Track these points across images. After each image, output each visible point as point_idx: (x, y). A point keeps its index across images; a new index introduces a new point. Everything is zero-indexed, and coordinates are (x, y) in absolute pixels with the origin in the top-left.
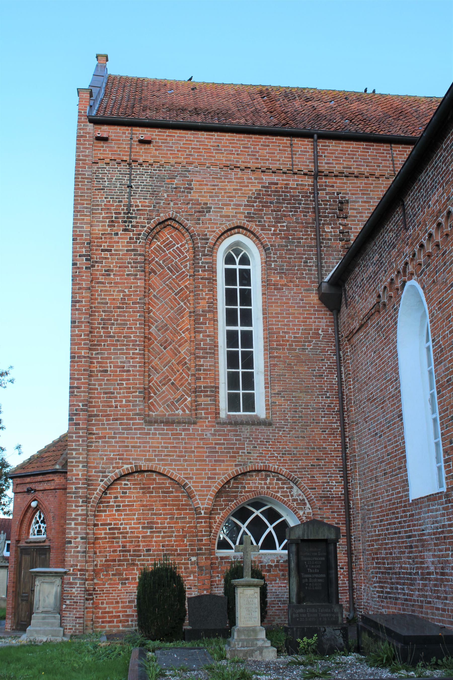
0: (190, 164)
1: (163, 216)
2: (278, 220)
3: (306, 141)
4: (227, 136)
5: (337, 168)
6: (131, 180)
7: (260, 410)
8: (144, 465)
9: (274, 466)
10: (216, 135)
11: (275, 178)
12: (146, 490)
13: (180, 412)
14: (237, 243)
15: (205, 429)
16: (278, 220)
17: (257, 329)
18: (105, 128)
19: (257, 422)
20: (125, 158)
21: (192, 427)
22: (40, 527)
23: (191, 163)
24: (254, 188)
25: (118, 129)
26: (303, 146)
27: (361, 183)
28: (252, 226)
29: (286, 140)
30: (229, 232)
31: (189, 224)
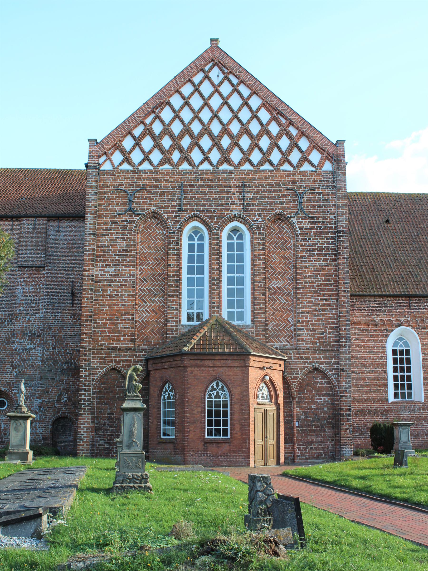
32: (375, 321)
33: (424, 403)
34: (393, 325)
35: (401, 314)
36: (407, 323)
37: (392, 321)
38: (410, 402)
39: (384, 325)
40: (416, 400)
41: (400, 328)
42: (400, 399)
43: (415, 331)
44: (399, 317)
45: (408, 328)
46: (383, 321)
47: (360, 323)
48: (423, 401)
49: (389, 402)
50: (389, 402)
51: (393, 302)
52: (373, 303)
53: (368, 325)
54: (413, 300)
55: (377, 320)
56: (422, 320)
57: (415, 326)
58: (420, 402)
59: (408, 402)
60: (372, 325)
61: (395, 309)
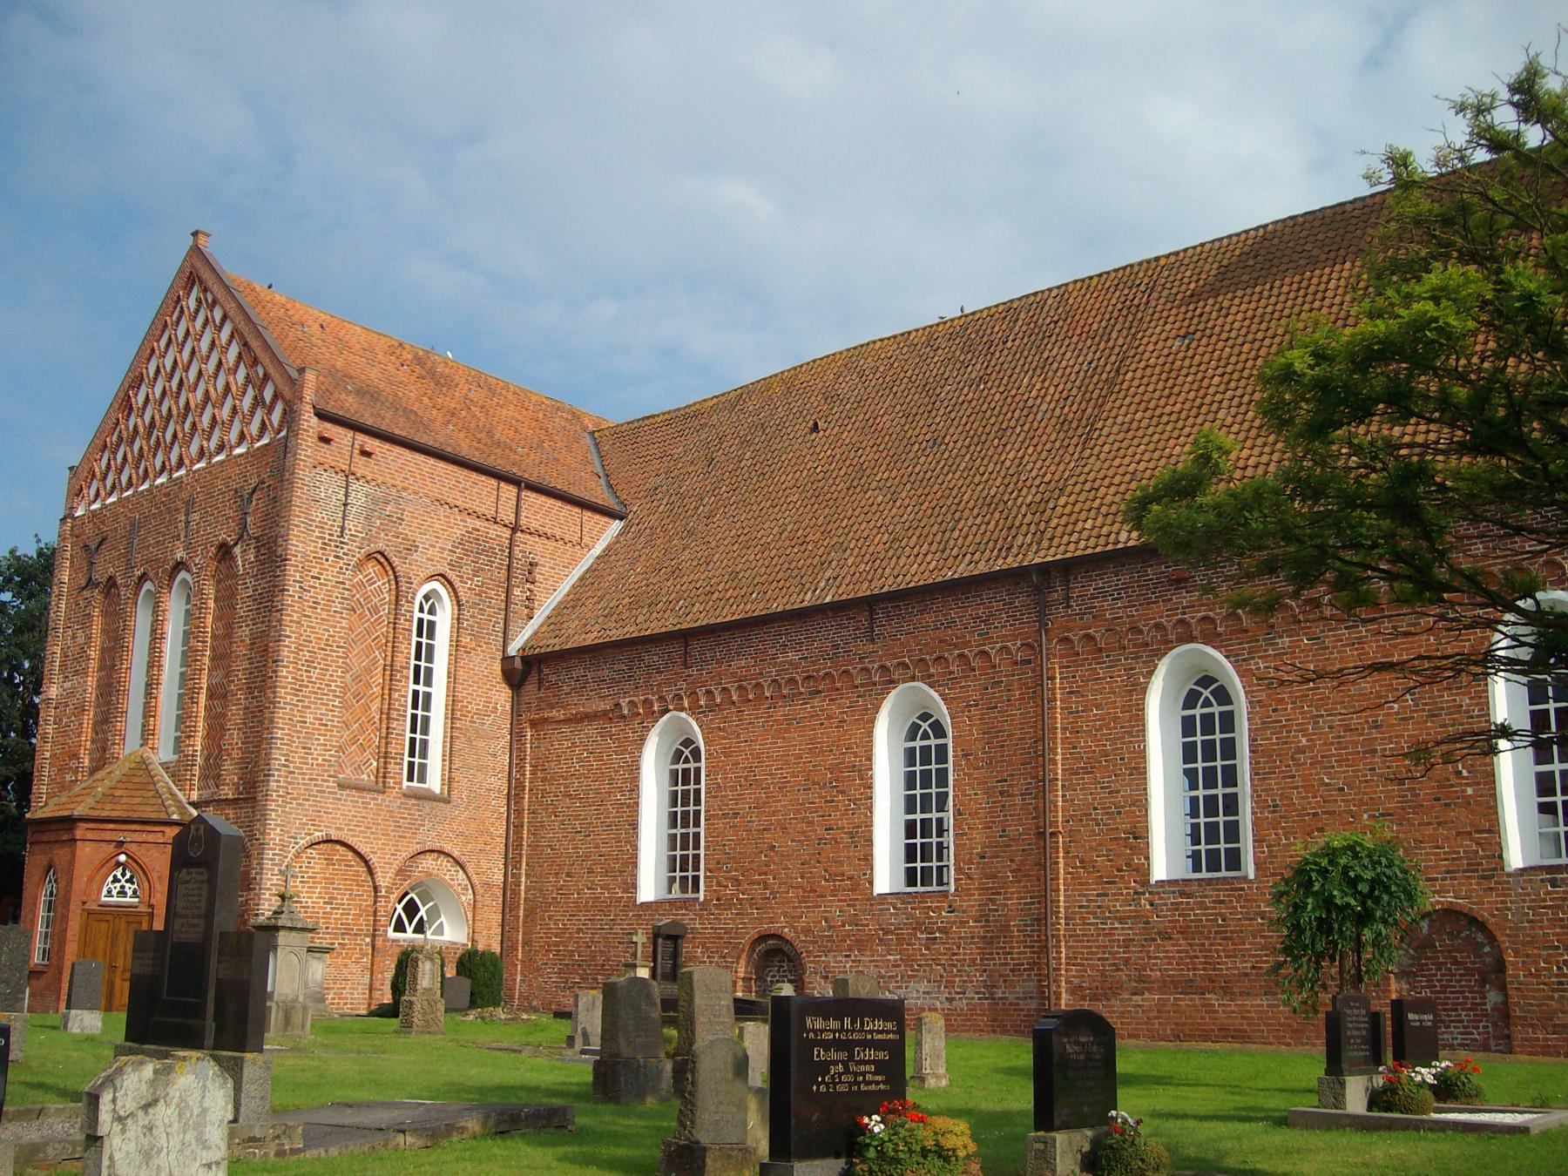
0: (405, 489)
1: (373, 547)
2: (476, 572)
3: (511, 488)
4: (442, 465)
5: (534, 525)
6: (346, 496)
7: (434, 782)
8: (335, 835)
9: (447, 848)
10: (432, 461)
11: (478, 524)
12: (330, 862)
13: (365, 777)
14: (434, 591)
15: (390, 800)
16: (476, 572)
17: (439, 691)
18: (328, 425)
19: (429, 797)
20: (345, 467)
21: (380, 797)
22: (123, 887)
23: (405, 489)
24: (458, 533)
25: (340, 430)
26: (509, 491)
27: (551, 544)
28: (452, 576)
29: (493, 482)
30: (430, 578)
31: (396, 561)
33: (702, 904)
35: (668, 682)
41: (668, 715)
45: (683, 715)
51: (654, 657)
54: (695, 645)
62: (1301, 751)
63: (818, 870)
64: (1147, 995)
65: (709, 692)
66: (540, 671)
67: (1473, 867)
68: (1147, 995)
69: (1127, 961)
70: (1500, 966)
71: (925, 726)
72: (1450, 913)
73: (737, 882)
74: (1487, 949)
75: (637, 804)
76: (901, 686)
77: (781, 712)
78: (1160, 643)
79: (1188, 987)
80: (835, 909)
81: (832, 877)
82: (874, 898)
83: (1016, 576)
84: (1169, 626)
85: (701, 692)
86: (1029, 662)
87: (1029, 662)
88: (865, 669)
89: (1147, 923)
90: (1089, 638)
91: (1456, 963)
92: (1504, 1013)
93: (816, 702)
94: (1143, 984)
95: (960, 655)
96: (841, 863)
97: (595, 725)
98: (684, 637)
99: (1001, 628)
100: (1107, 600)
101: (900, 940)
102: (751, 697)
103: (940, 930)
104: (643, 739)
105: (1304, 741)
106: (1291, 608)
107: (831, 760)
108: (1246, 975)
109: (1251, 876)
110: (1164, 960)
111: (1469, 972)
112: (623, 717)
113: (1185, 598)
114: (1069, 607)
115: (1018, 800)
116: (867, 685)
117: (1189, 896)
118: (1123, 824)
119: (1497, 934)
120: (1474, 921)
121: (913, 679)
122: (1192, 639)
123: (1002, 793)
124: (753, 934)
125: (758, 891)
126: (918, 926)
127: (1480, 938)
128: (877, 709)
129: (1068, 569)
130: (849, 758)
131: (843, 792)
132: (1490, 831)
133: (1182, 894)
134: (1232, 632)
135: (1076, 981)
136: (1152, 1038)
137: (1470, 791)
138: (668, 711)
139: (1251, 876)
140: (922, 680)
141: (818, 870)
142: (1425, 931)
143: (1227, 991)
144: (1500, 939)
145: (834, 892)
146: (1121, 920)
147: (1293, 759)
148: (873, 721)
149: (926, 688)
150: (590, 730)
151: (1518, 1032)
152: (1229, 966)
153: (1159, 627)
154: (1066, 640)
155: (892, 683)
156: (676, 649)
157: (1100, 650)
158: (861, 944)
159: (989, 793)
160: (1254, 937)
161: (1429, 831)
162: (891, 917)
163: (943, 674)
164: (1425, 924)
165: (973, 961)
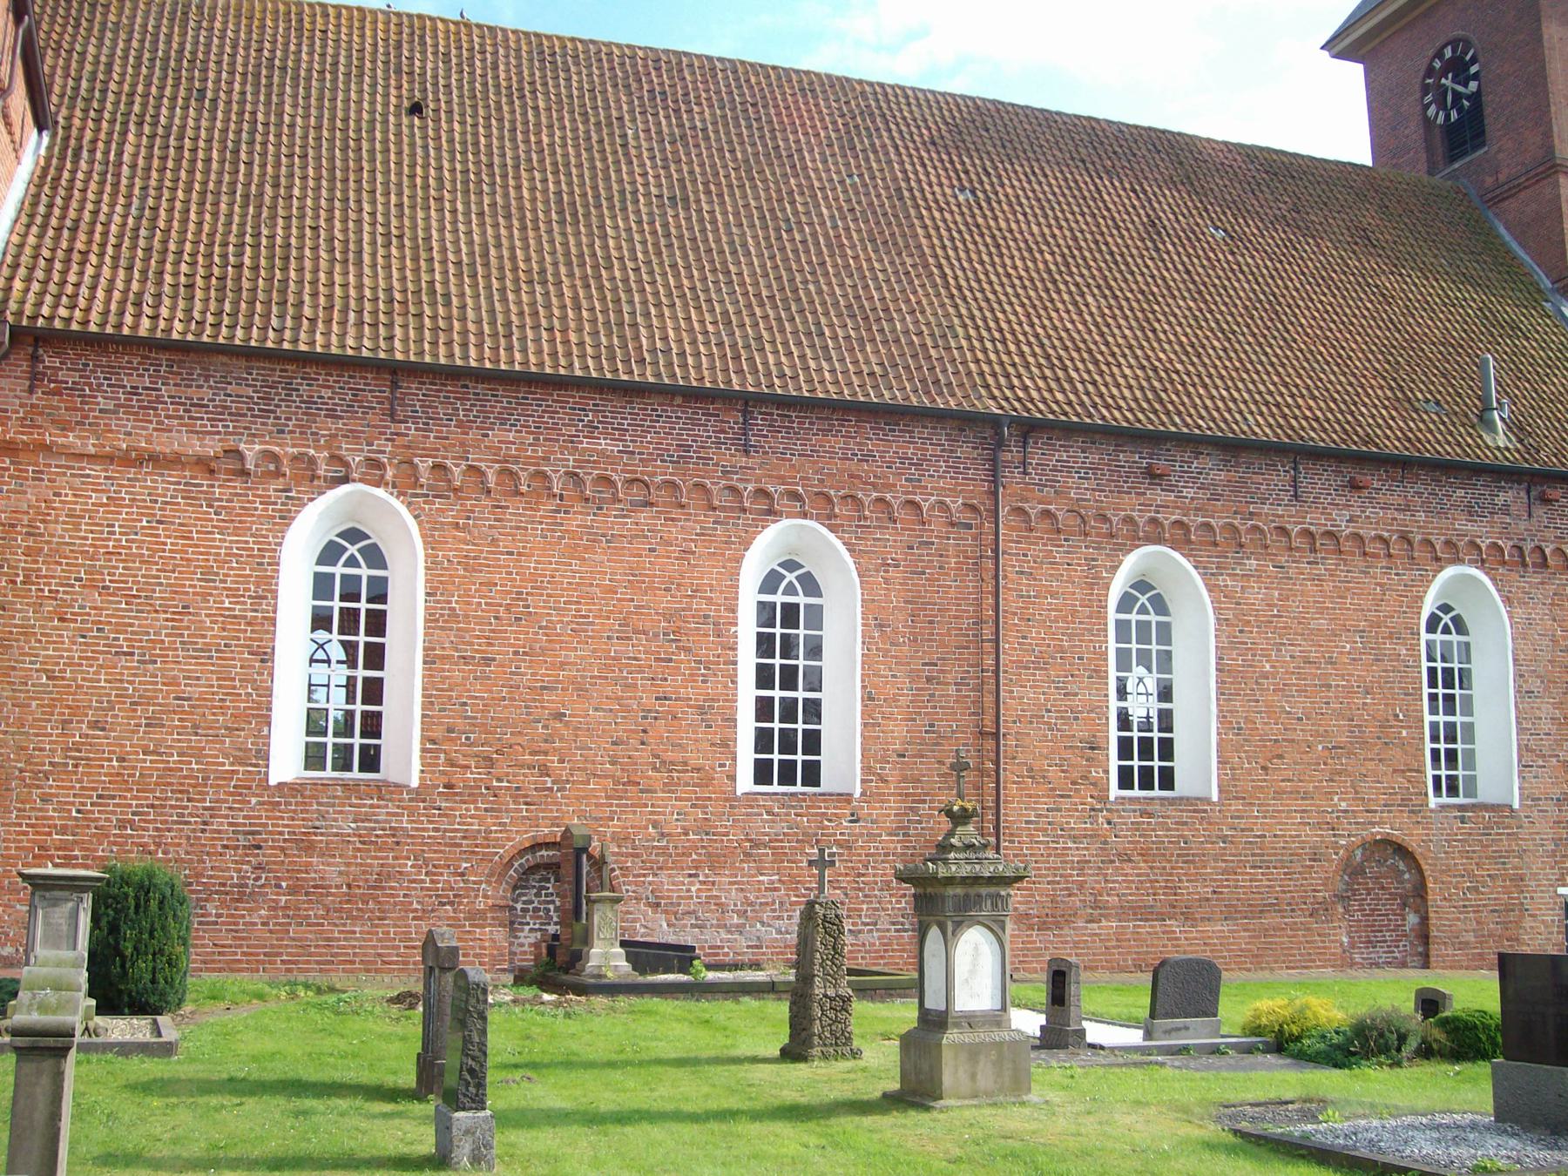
32: (240, 456)
33: (417, 791)
34: (311, 479)
35: (353, 435)
36: (374, 472)
37: (312, 461)
38: (367, 783)
39: (278, 474)
40: (392, 779)
42: (330, 773)
43: (409, 505)
44: (345, 448)
45: (380, 492)
46: (274, 458)
47: (174, 461)
48: (415, 783)
49: (273, 781)
50: (273, 781)
51: (326, 389)
52: (247, 386)
53: (212, 472)
55: (251, 451)
56: (436, 466)
57: (406, 485)
58: (400, 787)
59: (350, 788)
60: (228, 472)
61: (332, 414)
62: (1265, 676)
63: (643, 755)
64: (1104, 923)
65: (439, 467)
66: (35, 358)
67: (1405, 802)
68: (1104, 923)
69: (1081, 885)
70: (1420, 890)
71: (790, 577)
72: (1387, 842)
73: (489, 762)
74: (1407, 876)
75: (273, 622)
76: (785, 523)
77: (574, 523)
78: (1125, 537)
79: (1143, 913)
80: (673, 811)
81: (667, 765)
82: (736, 799)
83: (964, 421)
84: (1141, 522)
85: (424, 465)
86: (969, 526)
87: (969, 526)
88: (733, 489)
89: (1106, 843)
90: (1047, 514)
91: (1383, 888)
92: (1424, 937)
93: (643, 516)
94: (1098, 910)
95: (880, 500)
96: (683, 748)
97: (173, 475)
98: (395, 372)
99: (944, 478)
100: (1071, 477)
101: (779, 856)
102: (524, 488)
103: (838, 843)
104: (287, 519)
105: (1268, 667)
106: (1262, 532)
107: (665, 602)
108: (1208, 900)
109: (1215, 798)
110: (1123, 883)
111: (1393, 896)
112: (244, 473)
113: (1159, 496)
114: (1025, 473)
115: (952, 690)
116: (732, 509)
117: (1150, 815)
118: (1080, 731)
119: (1422, 862)
120: (1401, 850)
121: (805, 515)
122: (1159, 540)
123: (929, 680)
124: (523, 838)
125: (529, 780)
126: (806, 839)
127: (1402, 866)
128: (746, 544)
129: (1029, 429)
130: (698, 604)
131: (687, 650)
132: (1418, 771)
133: (1144, 813)
134: (1201, 543)
135: (1022, 908)
136: (1112, 970)
137: (1404, 733)
138: (345, 480)
139: (1215, 798)
140: (818, 518)
141: (643, 755)
142: (1358, 858)
143: (1188, 917)
144: (1425, 867)
145: (669, 786)
146: (1075, 839)
147: (1257, 683)
148: (739, 560)
149: (824, 531)
150: (163, 484)
151: (1434, 950)
152: (1188, 890)
153: (1129, 520)
154: (1020, 511)
155: (772, 513)
156: (374, 390)
157: (1059, 531)
158: (715, 861)
159: (914, 676)
160: (1216, 861)
161: (1371, 765)
162: (763, 826)
163: (850, 518)
164: (1359, 853)
165: (888, 883)
